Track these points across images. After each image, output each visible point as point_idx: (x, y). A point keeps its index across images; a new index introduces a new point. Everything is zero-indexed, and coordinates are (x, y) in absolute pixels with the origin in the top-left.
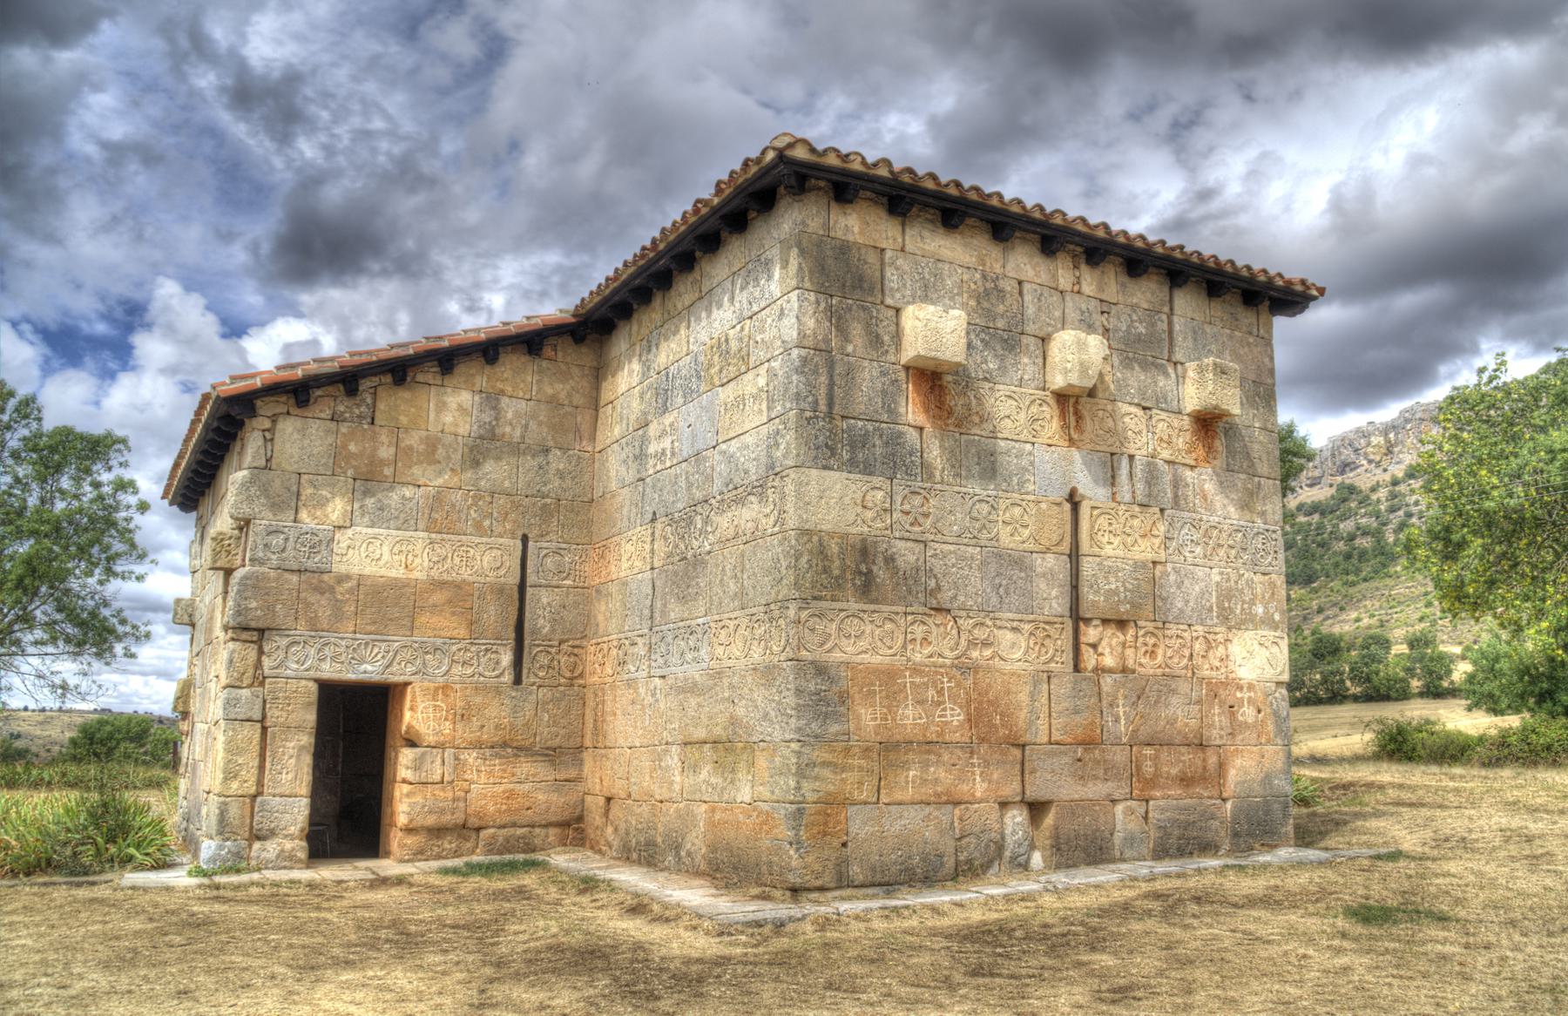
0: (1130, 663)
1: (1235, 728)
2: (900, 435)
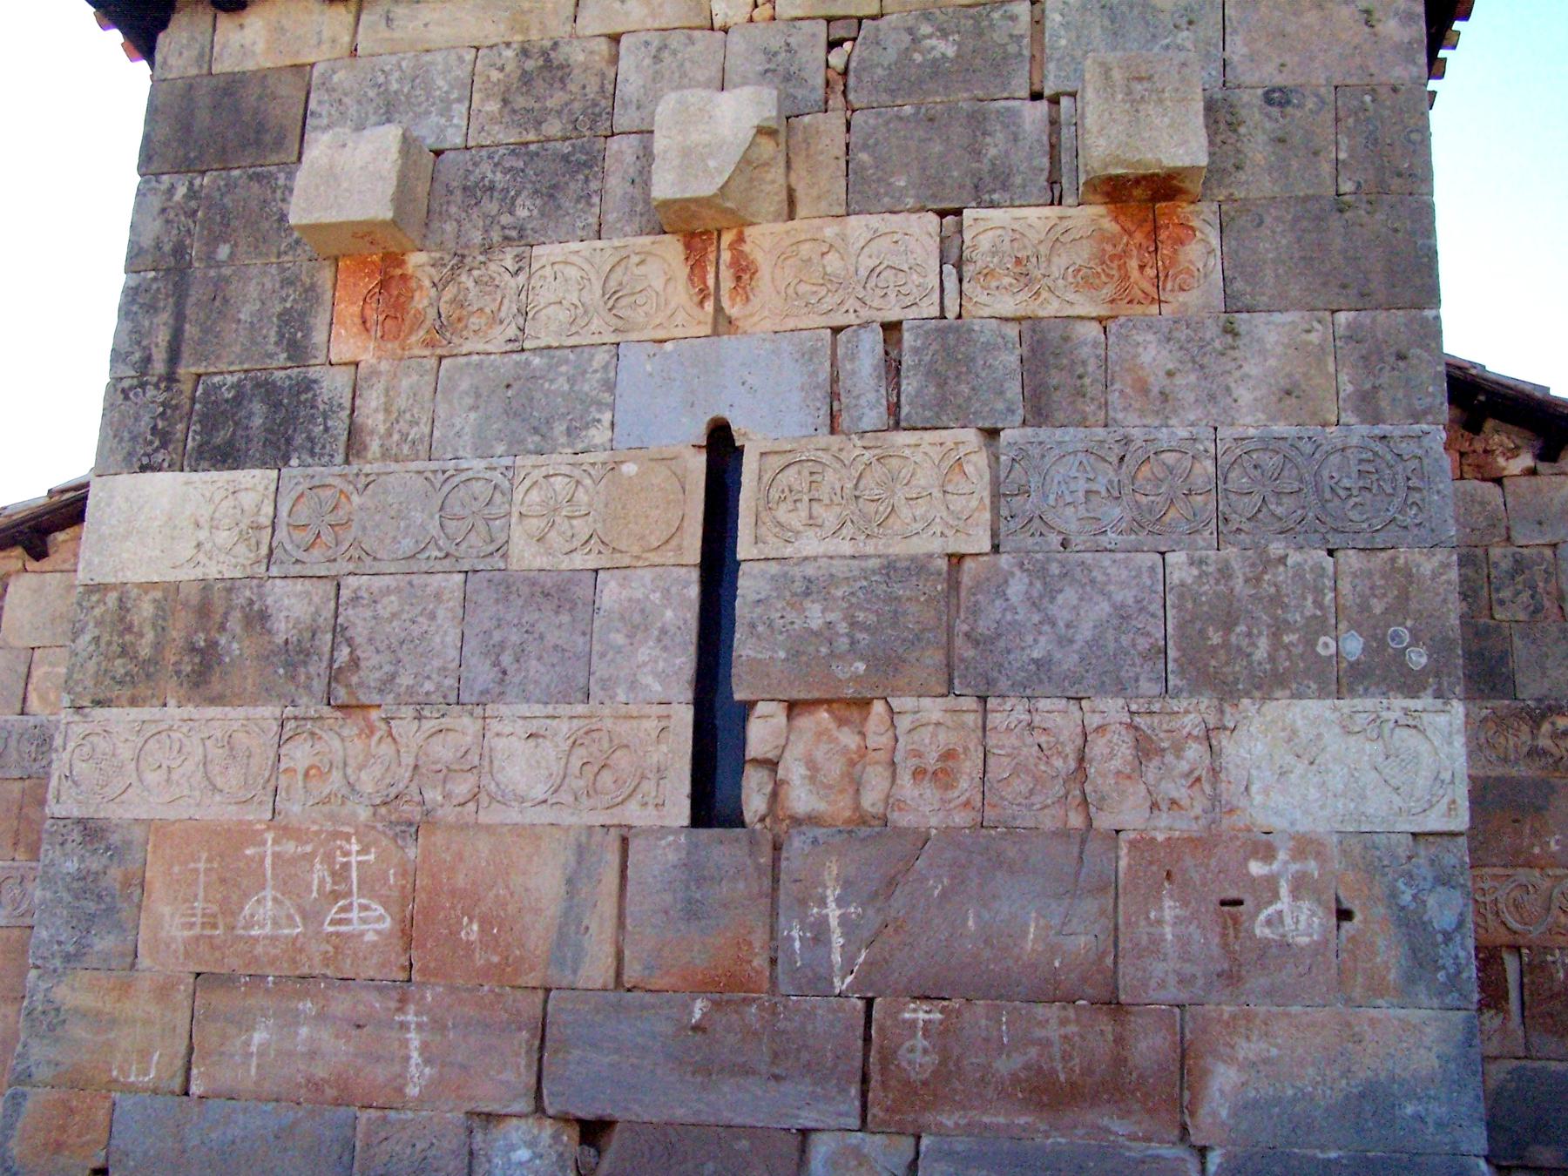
0: (871, 800)
2: (308, 385)
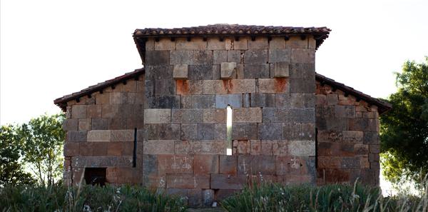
0: (248, 152)
1: (290, 170)
2: (174, 97)
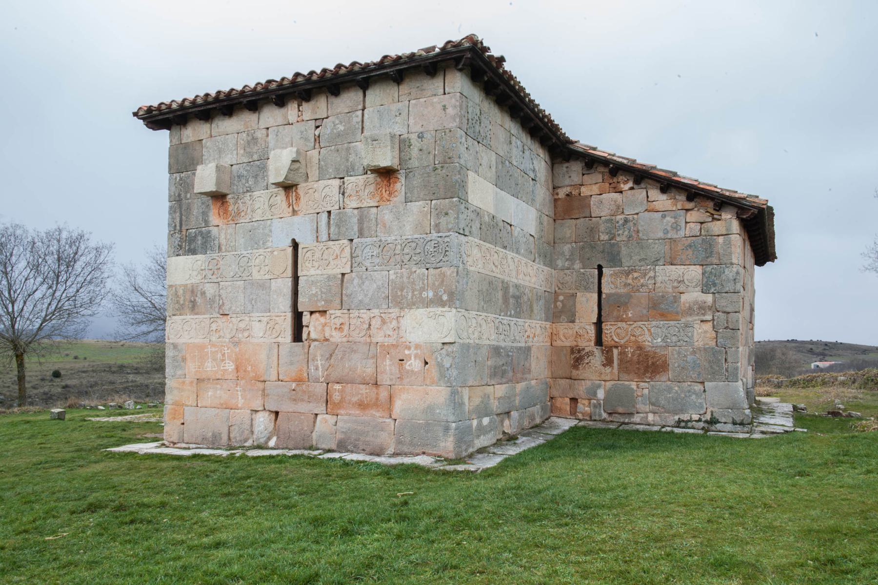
0: (327, 335)
